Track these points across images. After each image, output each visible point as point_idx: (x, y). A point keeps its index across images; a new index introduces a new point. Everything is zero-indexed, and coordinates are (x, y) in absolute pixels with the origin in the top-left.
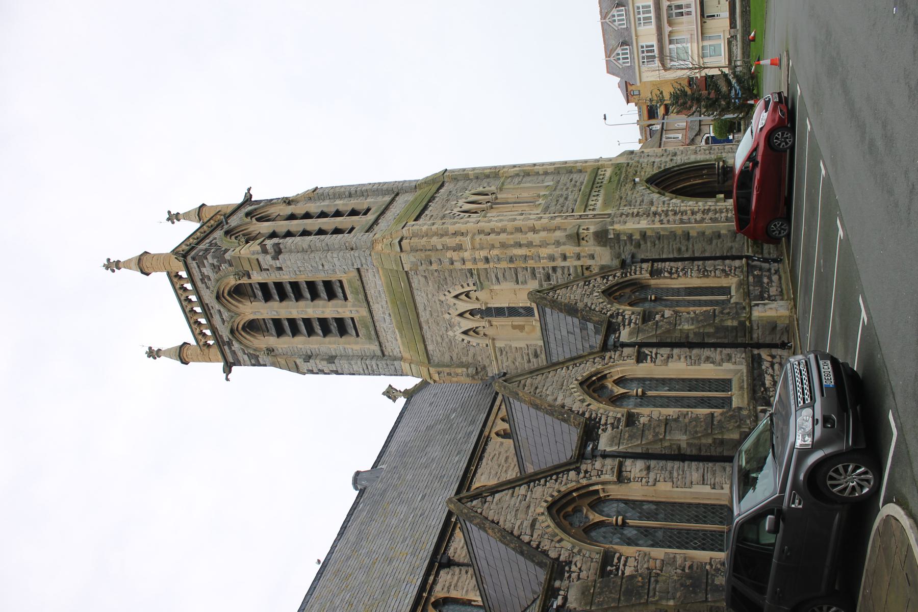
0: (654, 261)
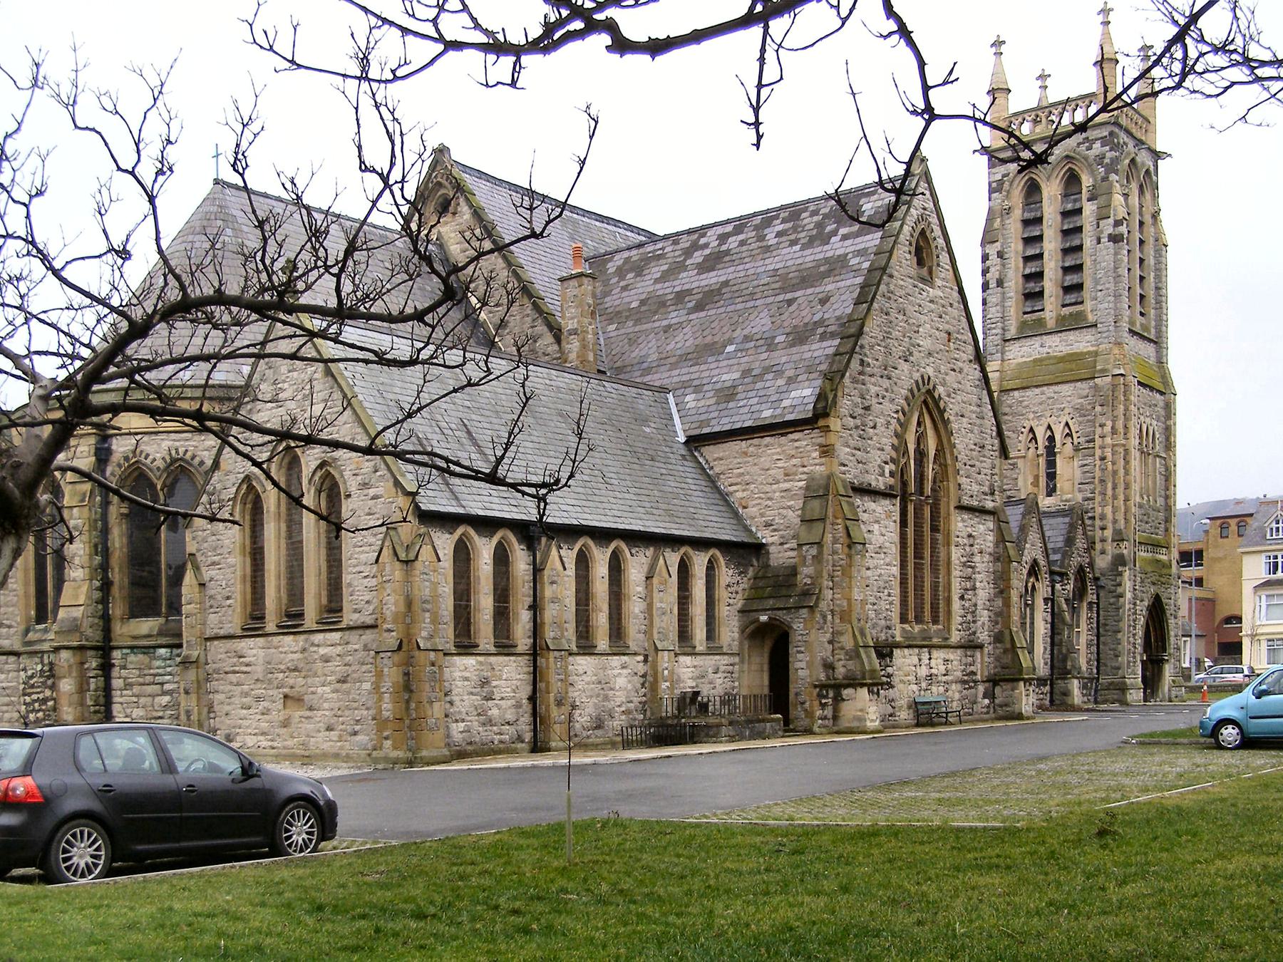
0: (1098, 604)
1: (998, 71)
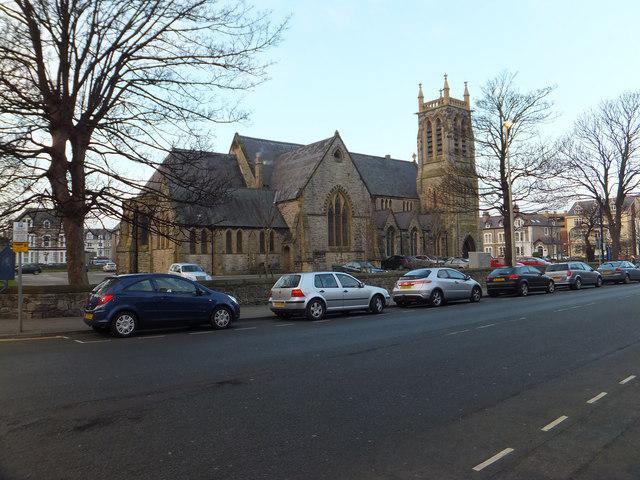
1: (421, 92)
